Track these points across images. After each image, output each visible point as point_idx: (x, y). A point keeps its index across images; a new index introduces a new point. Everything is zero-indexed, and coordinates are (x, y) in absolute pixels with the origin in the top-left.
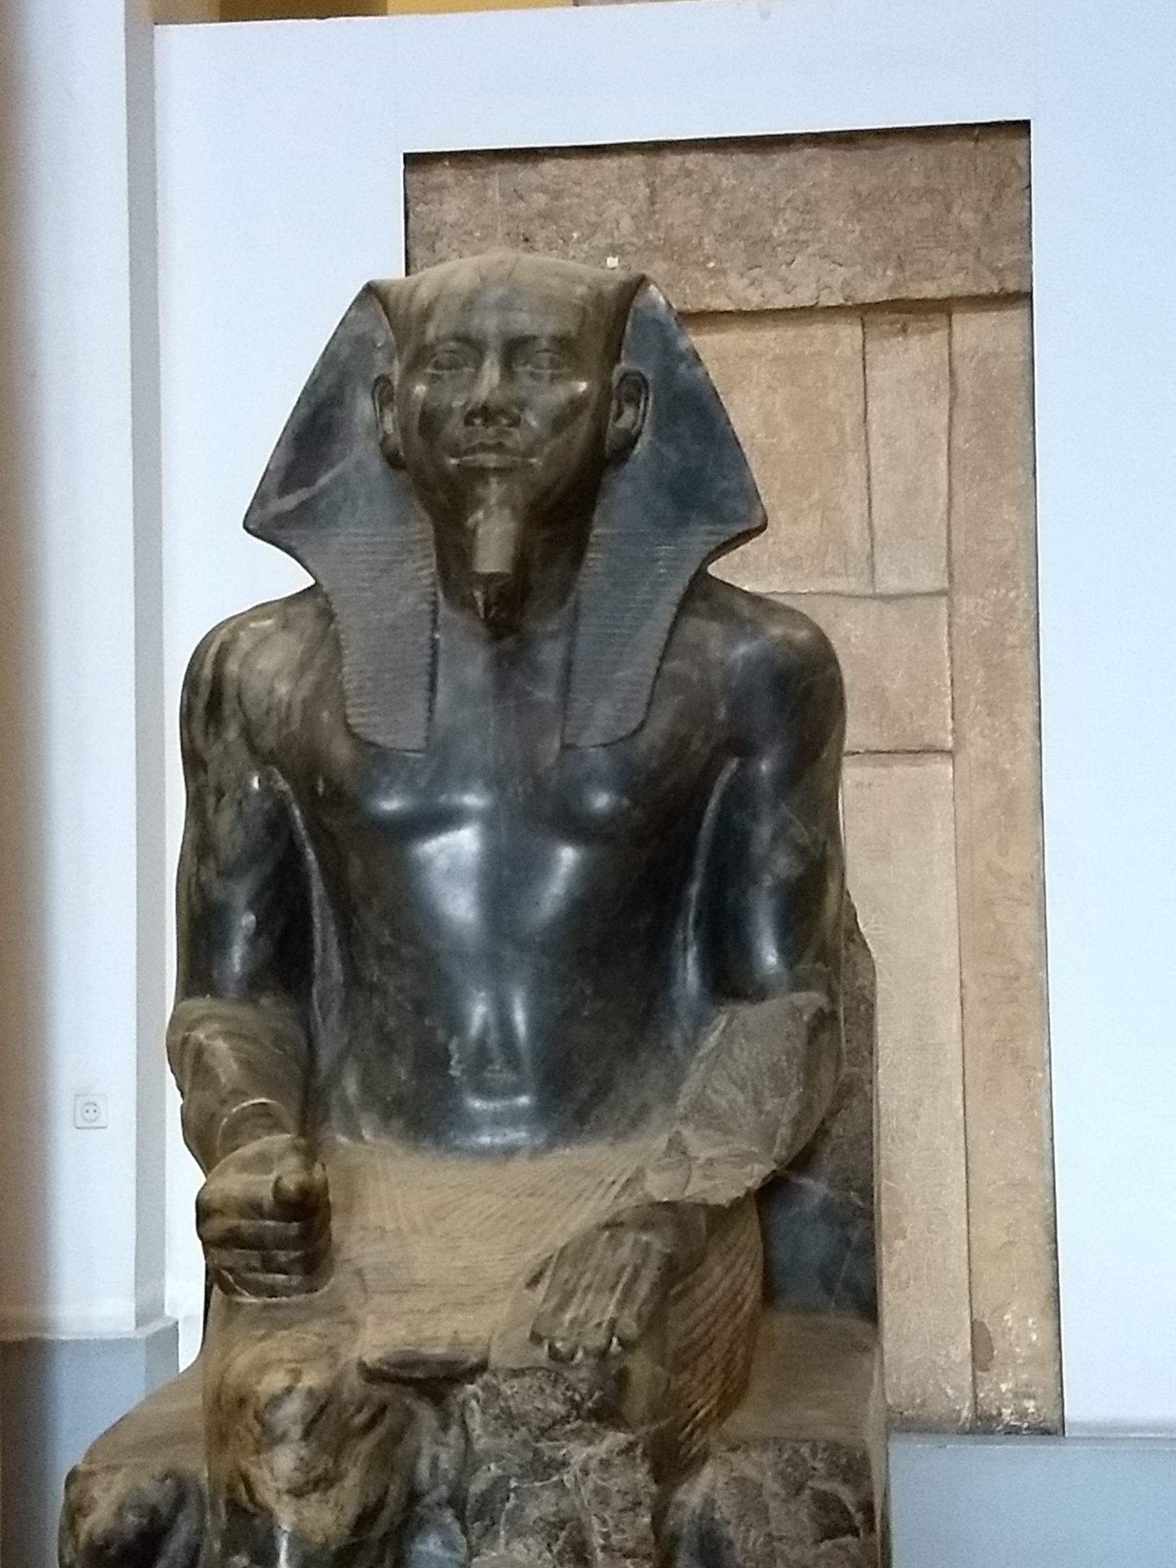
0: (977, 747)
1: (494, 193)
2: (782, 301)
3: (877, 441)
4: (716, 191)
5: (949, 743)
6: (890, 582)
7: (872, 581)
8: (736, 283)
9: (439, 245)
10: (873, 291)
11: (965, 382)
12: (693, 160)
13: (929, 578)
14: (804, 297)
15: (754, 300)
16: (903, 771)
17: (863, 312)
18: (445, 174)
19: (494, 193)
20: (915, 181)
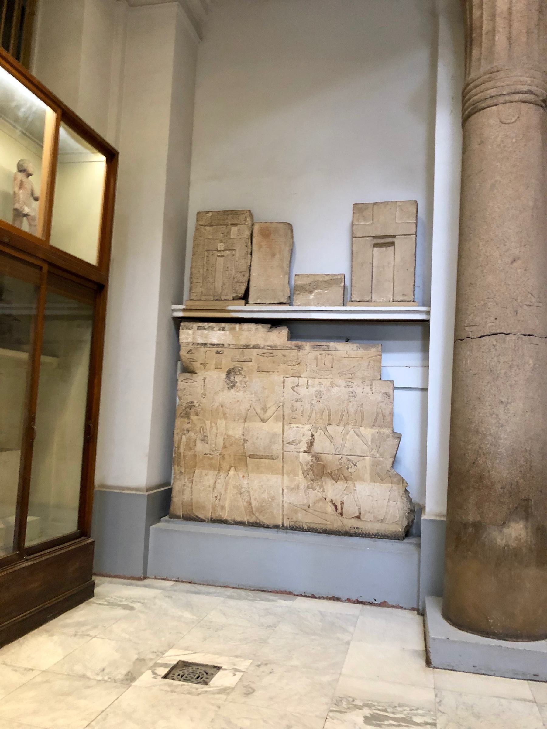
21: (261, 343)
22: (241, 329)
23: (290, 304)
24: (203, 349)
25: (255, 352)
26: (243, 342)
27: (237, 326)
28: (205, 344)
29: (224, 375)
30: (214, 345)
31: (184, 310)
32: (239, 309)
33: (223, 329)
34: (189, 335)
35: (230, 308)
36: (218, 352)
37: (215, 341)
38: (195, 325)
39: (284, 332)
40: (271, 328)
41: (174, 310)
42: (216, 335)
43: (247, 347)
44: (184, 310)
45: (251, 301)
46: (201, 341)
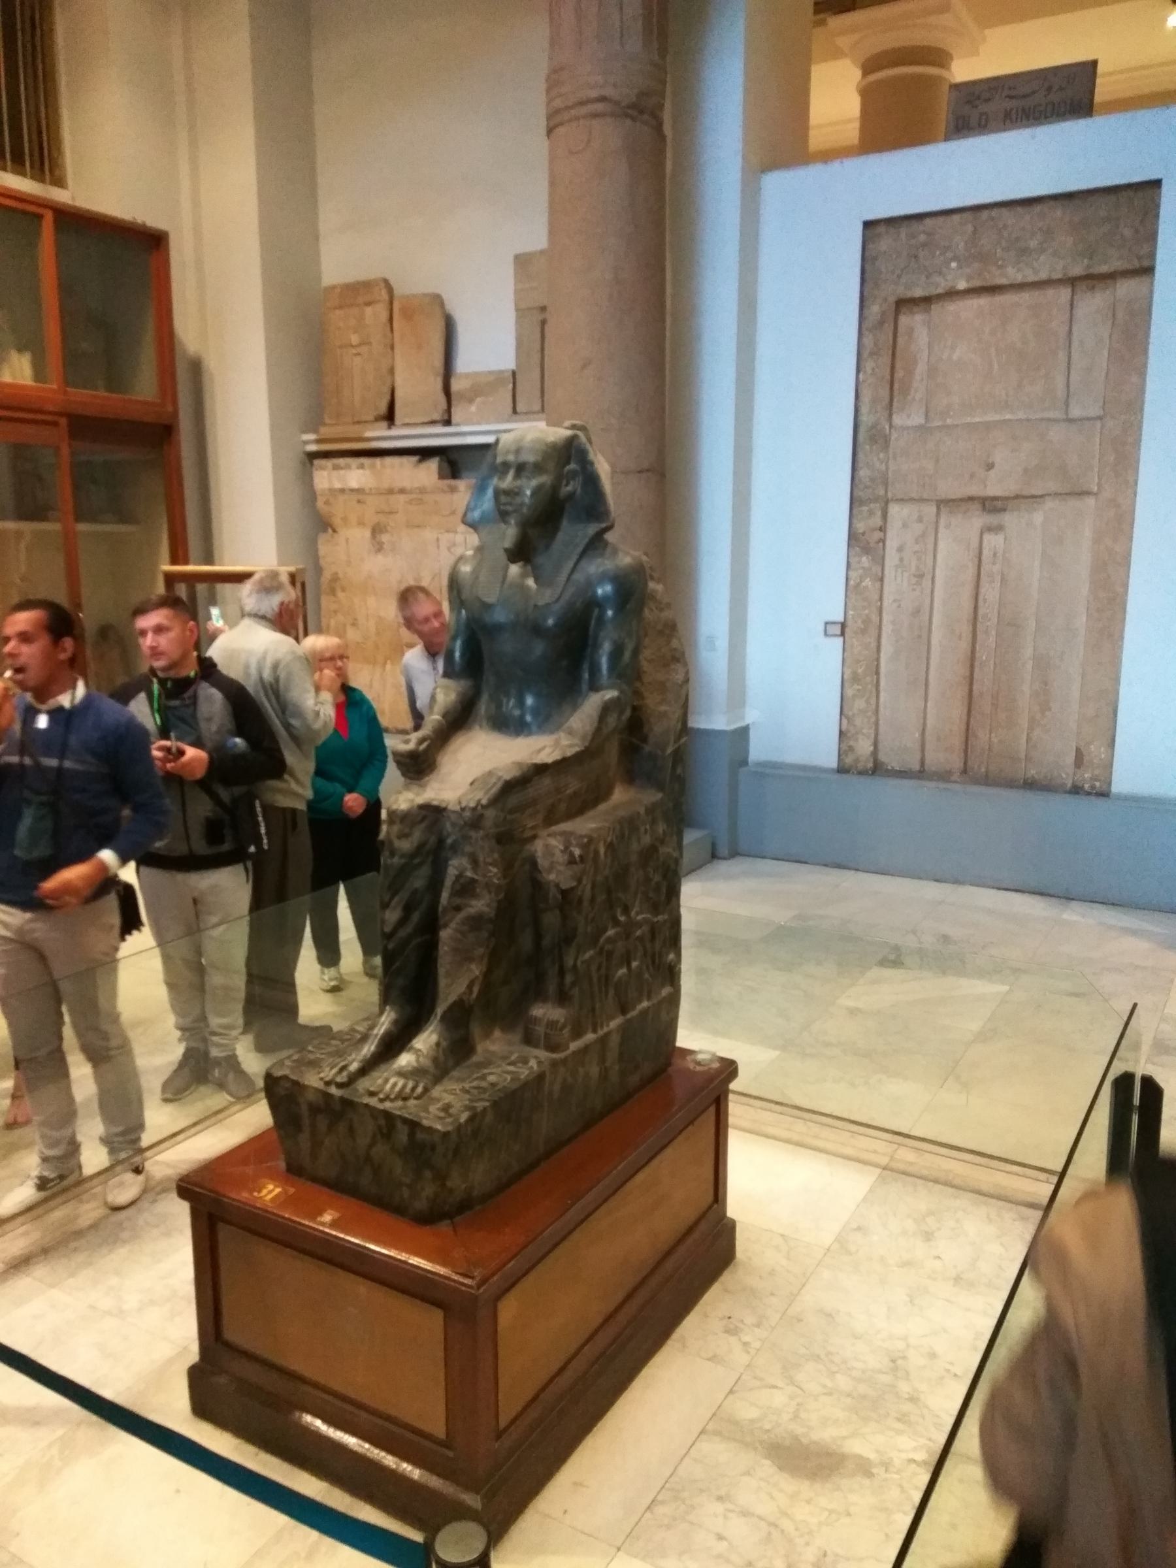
0: (1107, 494)
1: (903, 236)
2: (1032, 278)
3: (1075, 344)
4: (1005, 226)
5: (1095, 489)
6: (1076, 412)
7: (1067, 413)
8: (1010, 271)
9: (877, 263)
10: (1077, 270)
11: (1120, 315)
12: (994, 213)
13: (1094, 411)
14: (1043, 276)
15: (1019, 278)
16: (1073, 503)
17: (1072, 282)
18: (881, 229)
19: (903, 236)
20: (1103, 213)
21: (407, 484)
22: (383, 466)
23: (448, 422)
24: (341, 498)
25: (402, 498)
26: (386, 485)
27: (378, 461)
28: (342, 491)
29: (367, 533)
30: (352, 490)
31: (318, 441)
32: (379, 435)
33: (362, 467)
34: (325, 477)
35: (369, 434)
36: (359, 501)
37: (354, 485)
38: (329, 463)
39: (433, 465)
40: (420, 461)
41: (306, 443)
42: (356, 475)
43: (391, 491)
44: (318, 441)
45: (398, 421)
46: (338, 485)
